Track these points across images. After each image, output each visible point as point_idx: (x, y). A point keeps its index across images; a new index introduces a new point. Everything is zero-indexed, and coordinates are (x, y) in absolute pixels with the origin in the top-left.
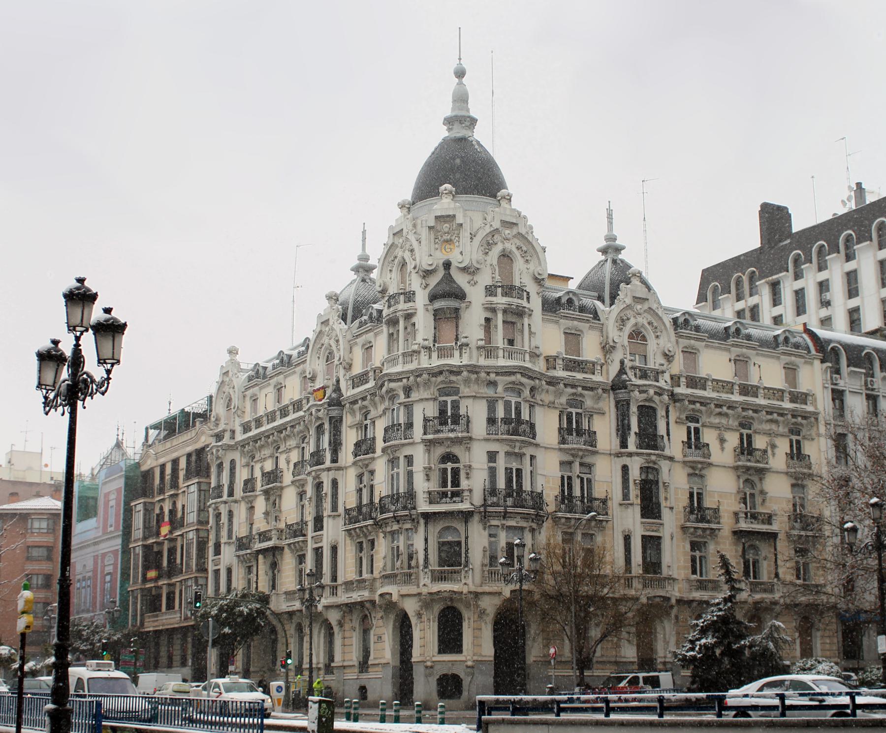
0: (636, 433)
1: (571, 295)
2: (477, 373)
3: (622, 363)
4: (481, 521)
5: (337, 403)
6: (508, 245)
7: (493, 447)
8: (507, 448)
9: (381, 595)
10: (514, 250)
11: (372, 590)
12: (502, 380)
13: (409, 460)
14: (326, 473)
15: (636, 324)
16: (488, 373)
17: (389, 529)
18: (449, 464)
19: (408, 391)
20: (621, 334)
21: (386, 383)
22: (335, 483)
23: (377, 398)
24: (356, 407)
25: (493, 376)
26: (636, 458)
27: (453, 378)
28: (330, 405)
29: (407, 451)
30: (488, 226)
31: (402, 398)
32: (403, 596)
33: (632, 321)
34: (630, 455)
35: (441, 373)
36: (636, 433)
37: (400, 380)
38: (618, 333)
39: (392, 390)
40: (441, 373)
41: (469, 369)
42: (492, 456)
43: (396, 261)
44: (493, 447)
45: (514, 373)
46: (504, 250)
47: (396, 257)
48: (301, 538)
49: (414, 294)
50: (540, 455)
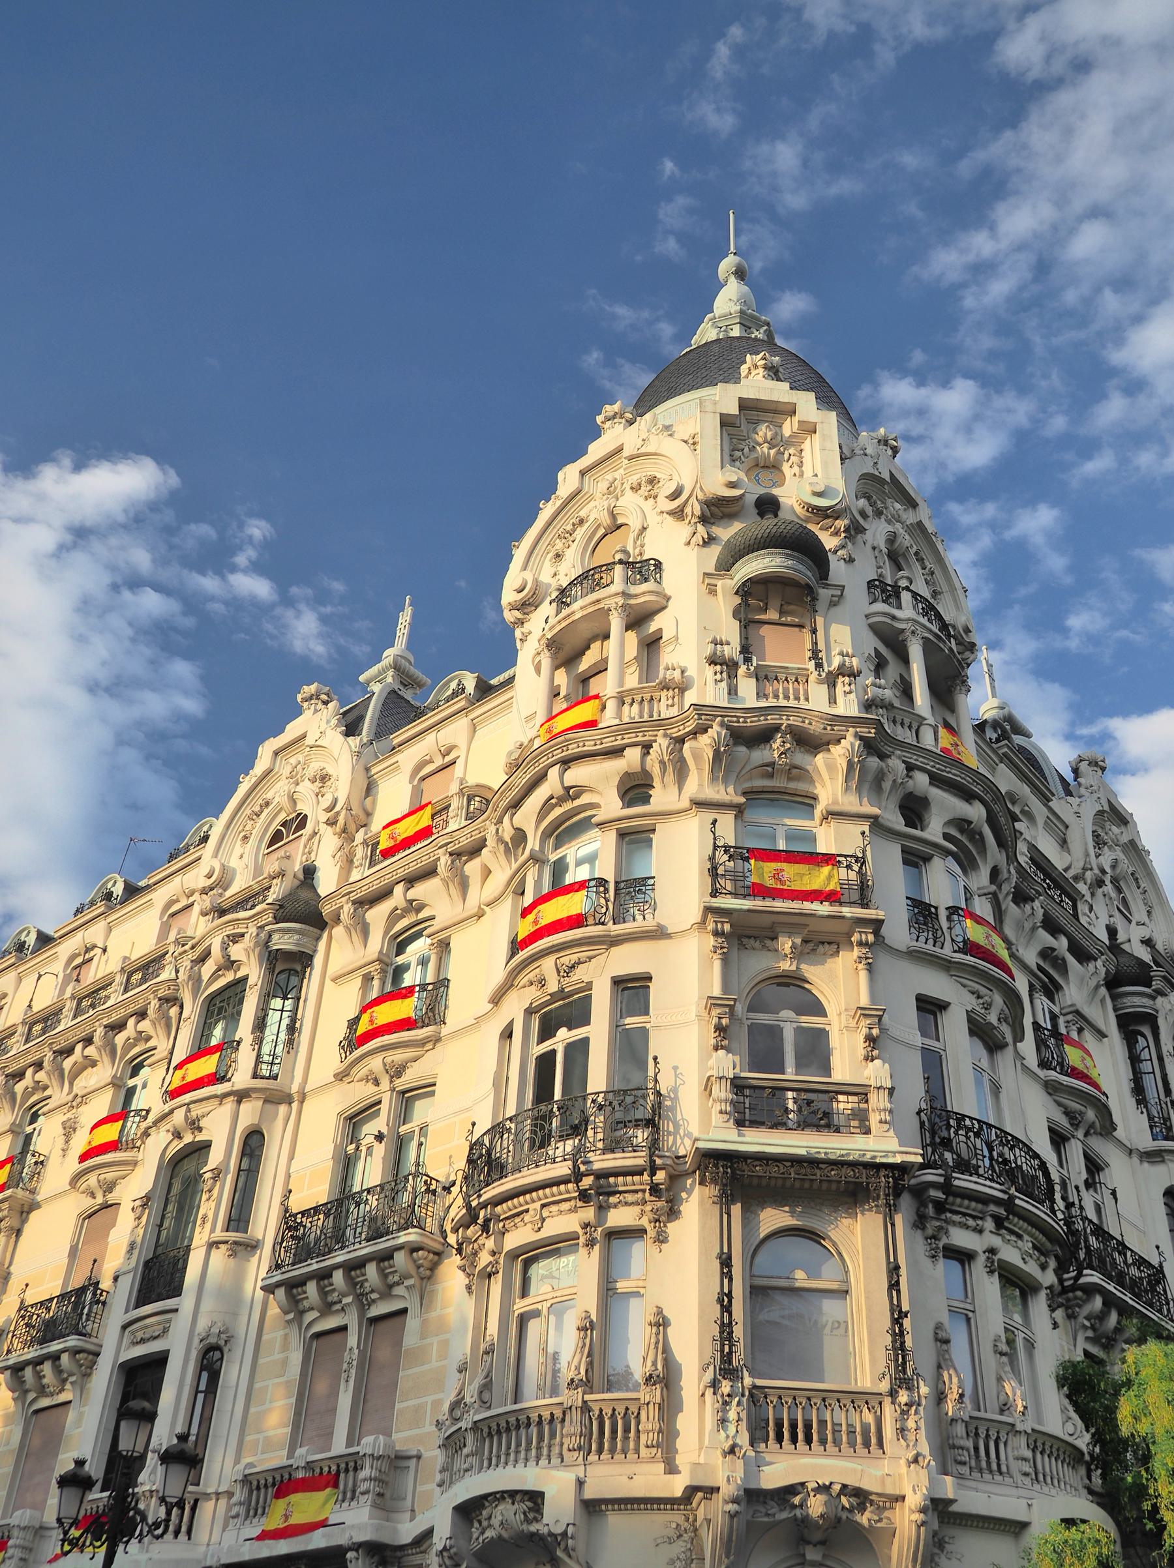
2: (882, 757)
4: (920, 1222)
5: (304, 910)
7: (938, 985)
8: (971, 1002)
9: (468, 1511)
11: (387, 1501)
12: (945, 808)
13: (633, 990)
14: (229, 1105)
16: (910, 768)
17: (518, 1237)
18: (787, 1014)
19: (635, 789)
21: (554, 773)
22: (253, 1144)
23: (472, 868)
24: (377, 915)
25: (922, 779)
28: (277, 920)
29: (626, 960)
31: (610, 805)
32: (592, 1508)
35: (764, 736)
37: (617, 752)
39: (570, 793)
40: (764, 736)
41: (864, 731)
43: (580, 532)
44: (938, 985)
47: (582, 522)
48: (72, 1341)
49: (658, 565)
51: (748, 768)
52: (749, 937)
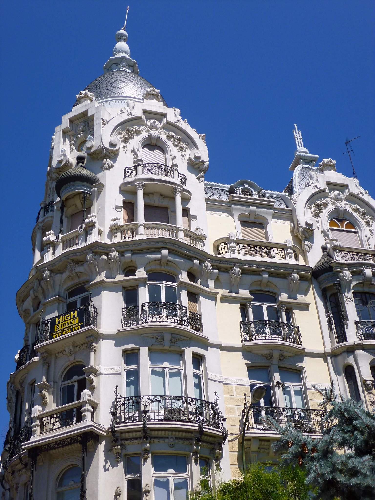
0: (356, 323)
1: (247, 186)
3: (324, 249)
6: (154, 133)
10: (163, 137)
15: (337, 210)
20: (319, 219)
26: (359, 352)
27: (79, 269)
30: (127, 113)
33: (331, 207)
34: (351, 350)
36: (356, 323)
38: (315, 219)
42: (131, 357)
45: (158, 250)
46: (150, 137)
50: (210, 355)
51: (63, 280)
52: (58, 353)
